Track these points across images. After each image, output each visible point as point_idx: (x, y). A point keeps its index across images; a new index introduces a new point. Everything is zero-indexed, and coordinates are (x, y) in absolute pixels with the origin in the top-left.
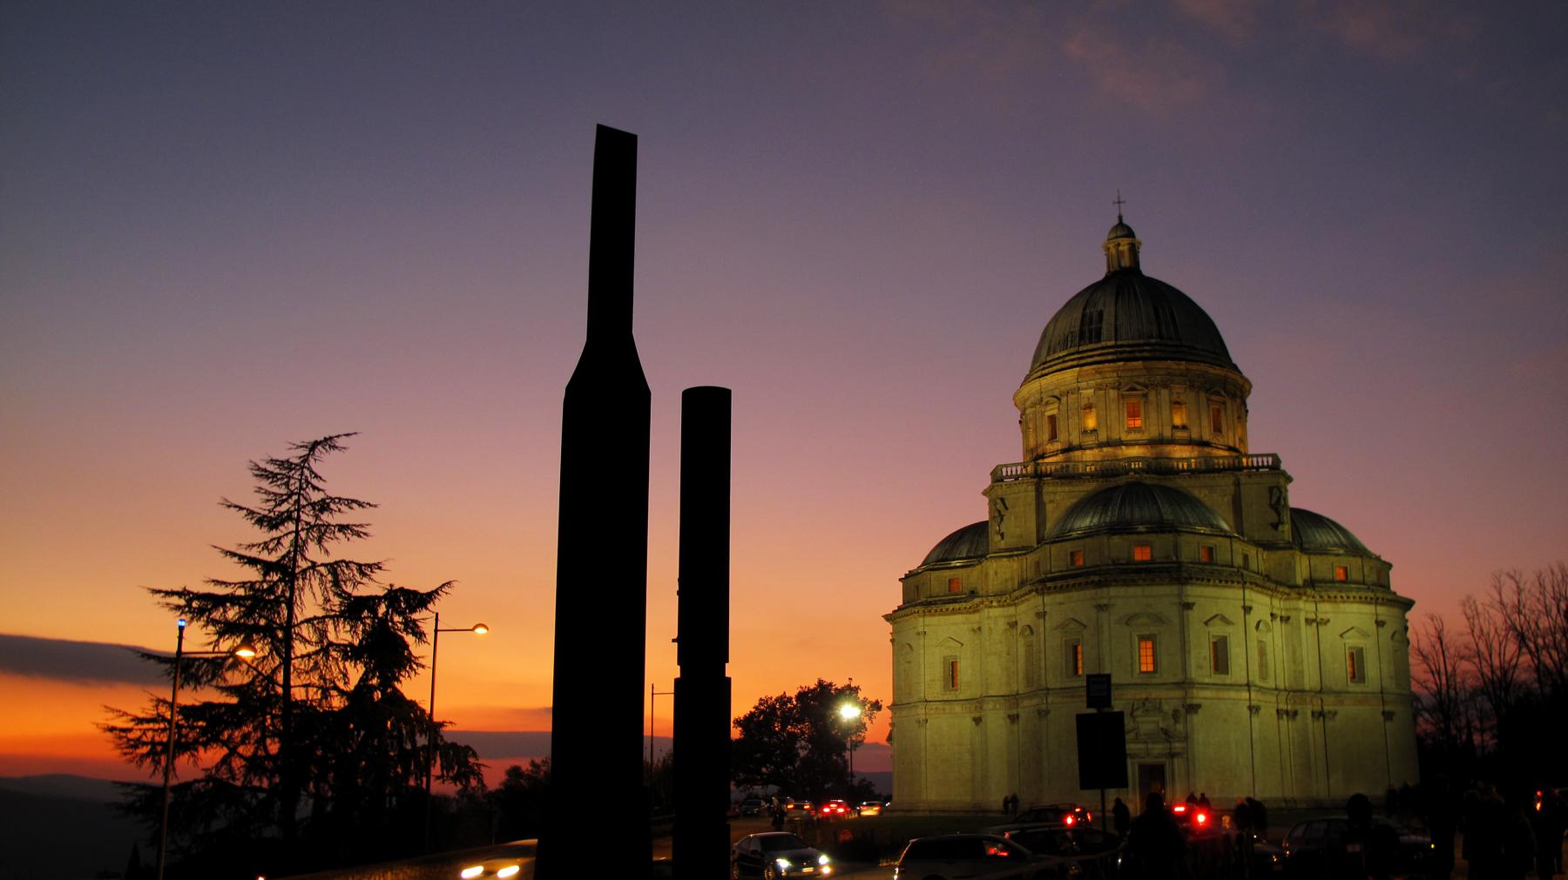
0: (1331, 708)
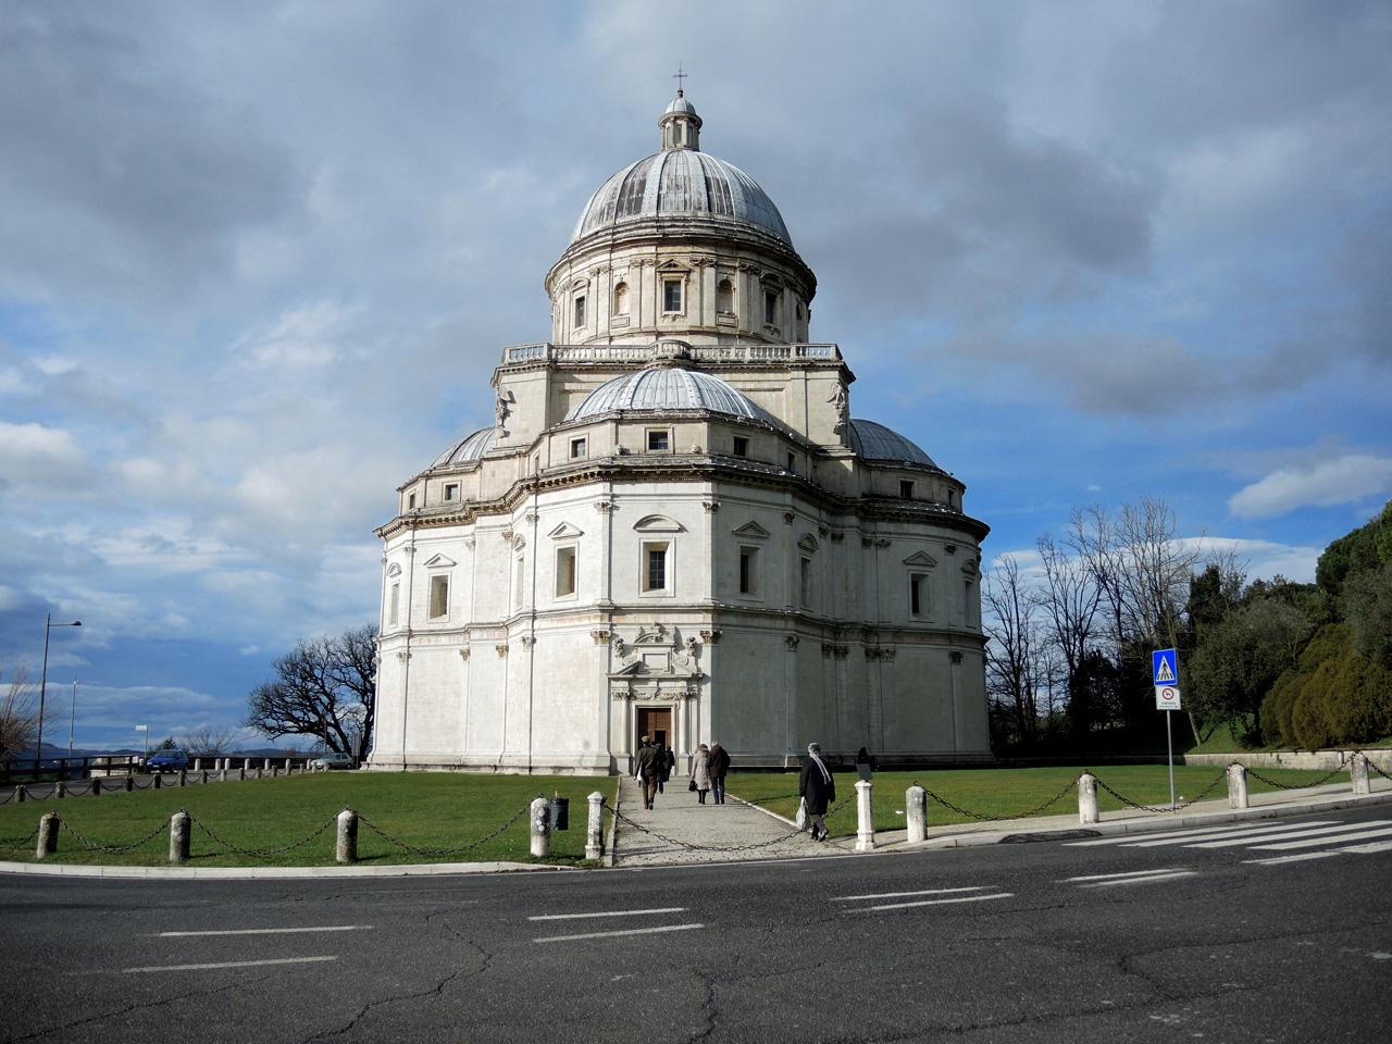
0: (890, 646)
